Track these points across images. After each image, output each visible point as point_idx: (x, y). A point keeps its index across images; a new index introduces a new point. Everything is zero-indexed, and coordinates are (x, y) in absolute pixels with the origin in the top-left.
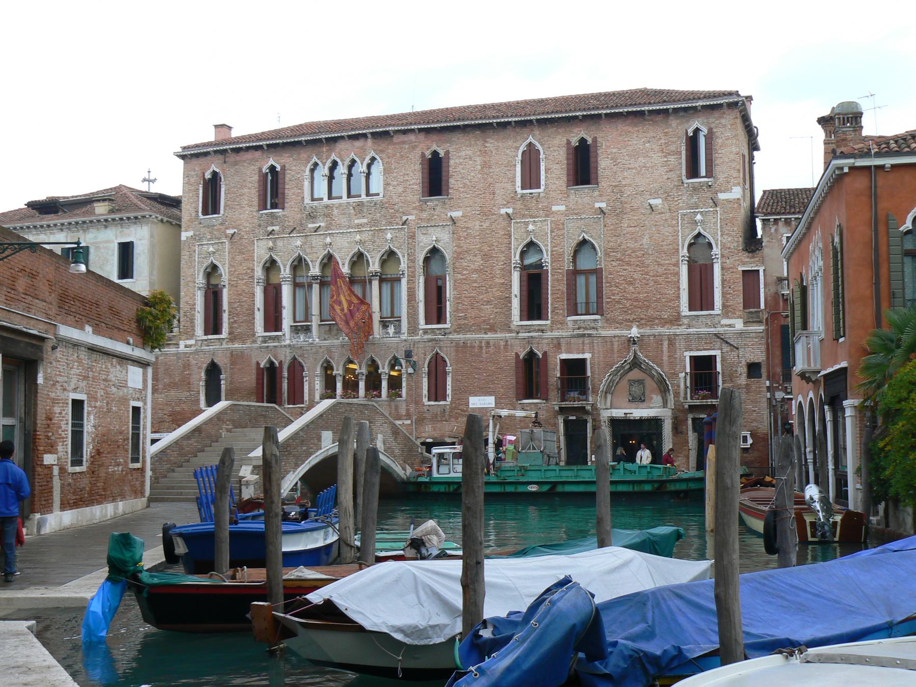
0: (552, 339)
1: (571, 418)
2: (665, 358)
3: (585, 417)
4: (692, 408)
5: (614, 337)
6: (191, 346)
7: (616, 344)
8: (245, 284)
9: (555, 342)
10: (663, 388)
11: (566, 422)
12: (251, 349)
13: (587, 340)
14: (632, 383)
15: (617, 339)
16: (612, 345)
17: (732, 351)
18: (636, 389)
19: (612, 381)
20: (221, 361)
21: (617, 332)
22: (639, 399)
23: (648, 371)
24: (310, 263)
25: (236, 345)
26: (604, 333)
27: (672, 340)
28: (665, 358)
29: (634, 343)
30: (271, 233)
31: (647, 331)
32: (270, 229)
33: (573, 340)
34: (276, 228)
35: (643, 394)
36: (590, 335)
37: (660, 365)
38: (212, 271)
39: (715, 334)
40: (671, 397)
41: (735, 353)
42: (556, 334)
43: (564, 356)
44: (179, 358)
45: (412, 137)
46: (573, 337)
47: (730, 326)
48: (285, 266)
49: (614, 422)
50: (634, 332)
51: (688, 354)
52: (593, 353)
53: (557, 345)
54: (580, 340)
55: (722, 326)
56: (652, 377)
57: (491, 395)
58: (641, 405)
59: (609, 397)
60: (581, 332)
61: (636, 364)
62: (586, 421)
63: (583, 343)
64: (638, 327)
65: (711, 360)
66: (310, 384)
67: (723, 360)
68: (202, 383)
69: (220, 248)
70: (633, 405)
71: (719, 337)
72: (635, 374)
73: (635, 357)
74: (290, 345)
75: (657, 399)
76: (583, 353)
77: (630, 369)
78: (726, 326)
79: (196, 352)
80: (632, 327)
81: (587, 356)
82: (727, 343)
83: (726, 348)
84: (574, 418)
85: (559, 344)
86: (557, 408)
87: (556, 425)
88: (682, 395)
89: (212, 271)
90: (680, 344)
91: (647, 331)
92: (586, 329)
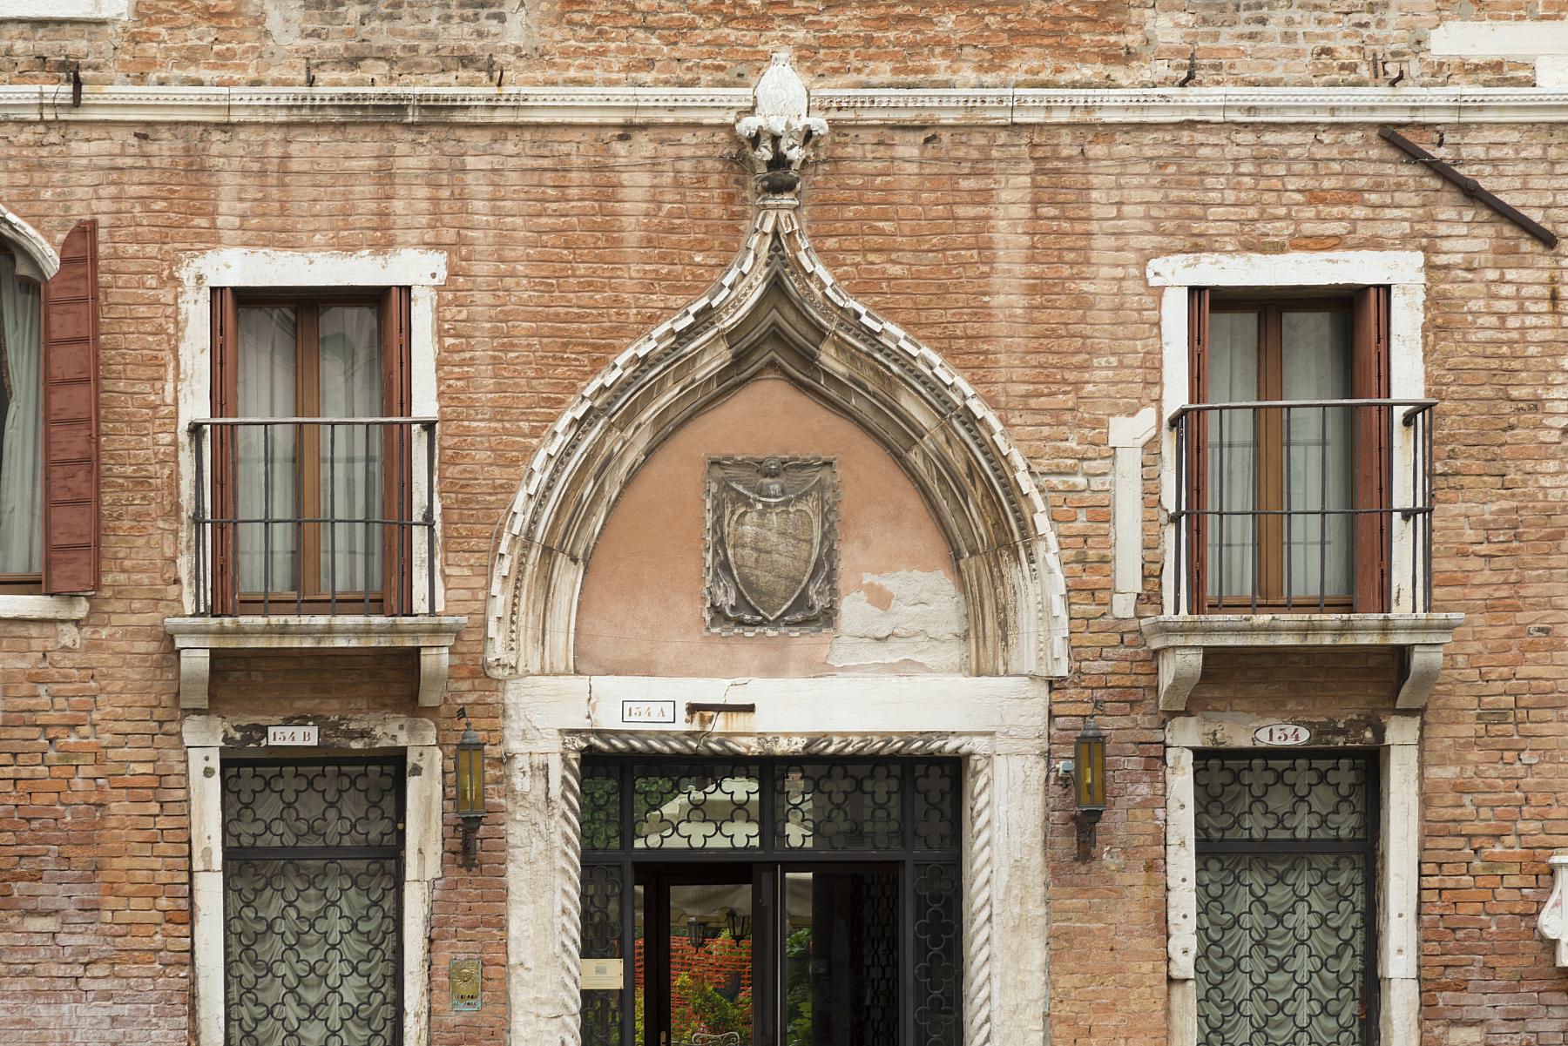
0: (145, 132)
1: (284, 736)
2: (1008, 299)
3: (391, 732)
4: (1229, 672)
5: (627, 131)
7: (636, 187)
9: (165, 148)
10: (976, 523)
11: (238, 767)
13: (413, 156)
14: (740, 480)
15: (643, 145)
16: (607, 192)
17: (1505, 254)
18: (769, 536)
19: (598, 465)
21: (653, 96)
22: (785, 608)
23: (873, 406)
26: (546, 98)
27: (1055, 160)
28: (1008, 299)
29: (779, 175)
31: (880, 93)
33: (304, 148)
35: (825, 568)
36: (437, 115)
37: (969, 351)
39: (1391, 135)
40: (1041, 589)
41: (1532, 273)
42: (174, 96)
43: (242, 267)
46: (305, 120)
47: (1496, 71)
49: (616, 775)
50: (783, 98)
51: (1178, 274)
52: (457, 249)
53: (184, 163)
54: (363, 149)
55: (1440, 72)
56: (895, 442)
58: (802, 642)
59: (568, 579)
60: (375, 83)
61: (779, 342)
62: (395, 765)
63: (385, 175)
64: (806, 57)
65: (1351, 313)
67: (1441, 321)
70: (748, 647)
71: (1412, 155)
72: (769, 417)
73: (776, 286)
75: (927, 594)
76: (384, 244)
77: (731, 380)
78: (1470, 70)
80: (757, 61)
81: (413, 268)
82: (1472, 193)
83: (1466, 237)
84: (305, 736)
85: (195, 168)
86: (196, 661)
87: (165, 789)
88: (1129, 577)
90: (1119, 195)
91: (880, 93)
92: (401, 62)
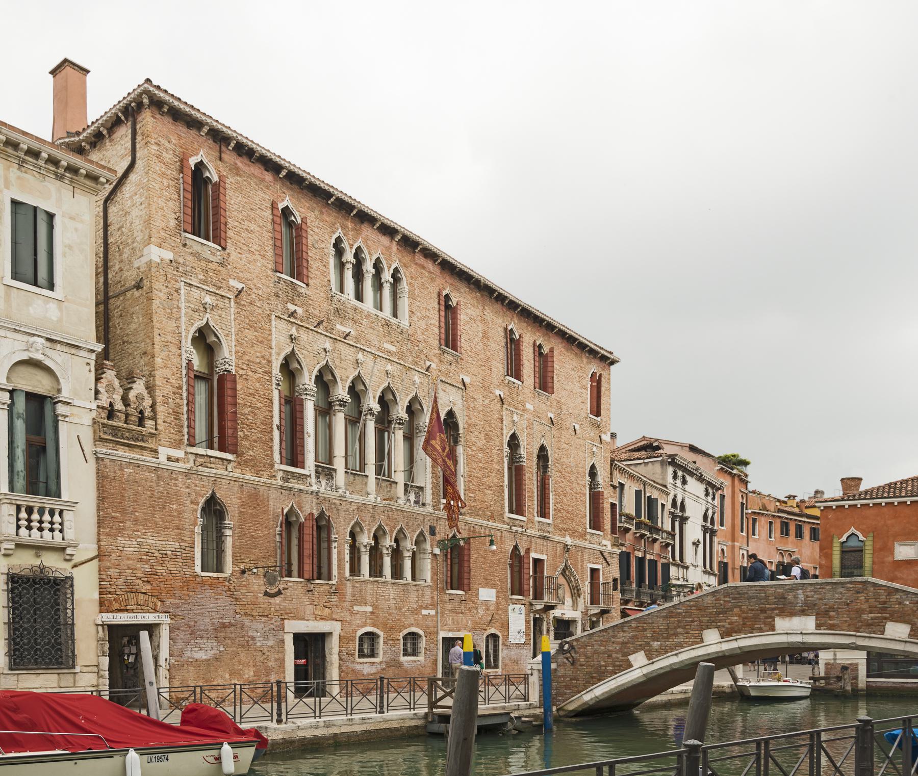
6: (177, 460)
8: (259, 380)
12: (269, 486)
20: (231, 501)
24: (338, 380)
25: (248, 476)
30: (292, 314)
32: (292, 308)
34: (300, 311)
38: (205, 341)
44: (159, 478)
45: (429, 265)
48: (311, 372)
57: (492, 588)
66: (339, 552)
68: (198, 530)
69: (221, 305)
74: (317, 493)
79: (188, 474)
89: (205, 341)
